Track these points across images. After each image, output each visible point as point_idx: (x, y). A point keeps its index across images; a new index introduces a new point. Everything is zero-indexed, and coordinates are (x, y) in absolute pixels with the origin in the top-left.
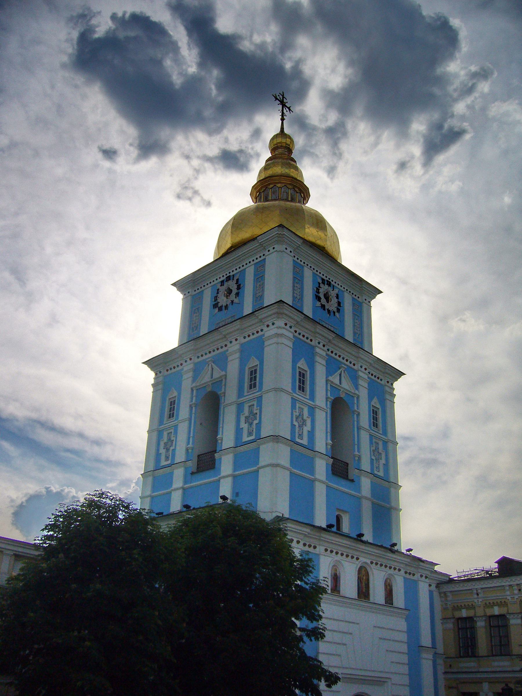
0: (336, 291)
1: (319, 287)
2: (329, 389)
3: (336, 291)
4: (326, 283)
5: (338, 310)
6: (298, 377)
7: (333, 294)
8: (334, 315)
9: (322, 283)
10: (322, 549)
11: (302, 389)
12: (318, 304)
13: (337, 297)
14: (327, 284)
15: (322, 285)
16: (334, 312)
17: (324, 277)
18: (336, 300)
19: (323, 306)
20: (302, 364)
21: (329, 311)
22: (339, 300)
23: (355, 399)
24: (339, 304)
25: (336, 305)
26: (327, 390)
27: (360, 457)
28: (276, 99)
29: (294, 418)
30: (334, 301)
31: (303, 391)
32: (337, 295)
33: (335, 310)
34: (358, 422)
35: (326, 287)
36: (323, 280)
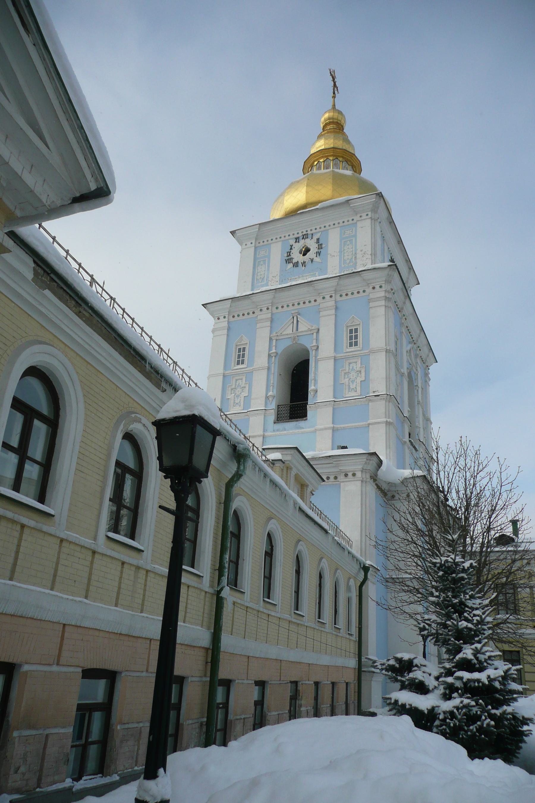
0: (315, 238)
2: (274, 344)
3: (315, 238)
7: (312, 244)
8: (312, 261)
9: (296, 242)
14: (303, 238)
16: (312, 260)
18: (317, 245)
19: (296, 265)
21: (304, 264)
22: (320, 243)
24: (320, 247)
32: (318, 240)
35: (302, 242)
36: (296, 239)
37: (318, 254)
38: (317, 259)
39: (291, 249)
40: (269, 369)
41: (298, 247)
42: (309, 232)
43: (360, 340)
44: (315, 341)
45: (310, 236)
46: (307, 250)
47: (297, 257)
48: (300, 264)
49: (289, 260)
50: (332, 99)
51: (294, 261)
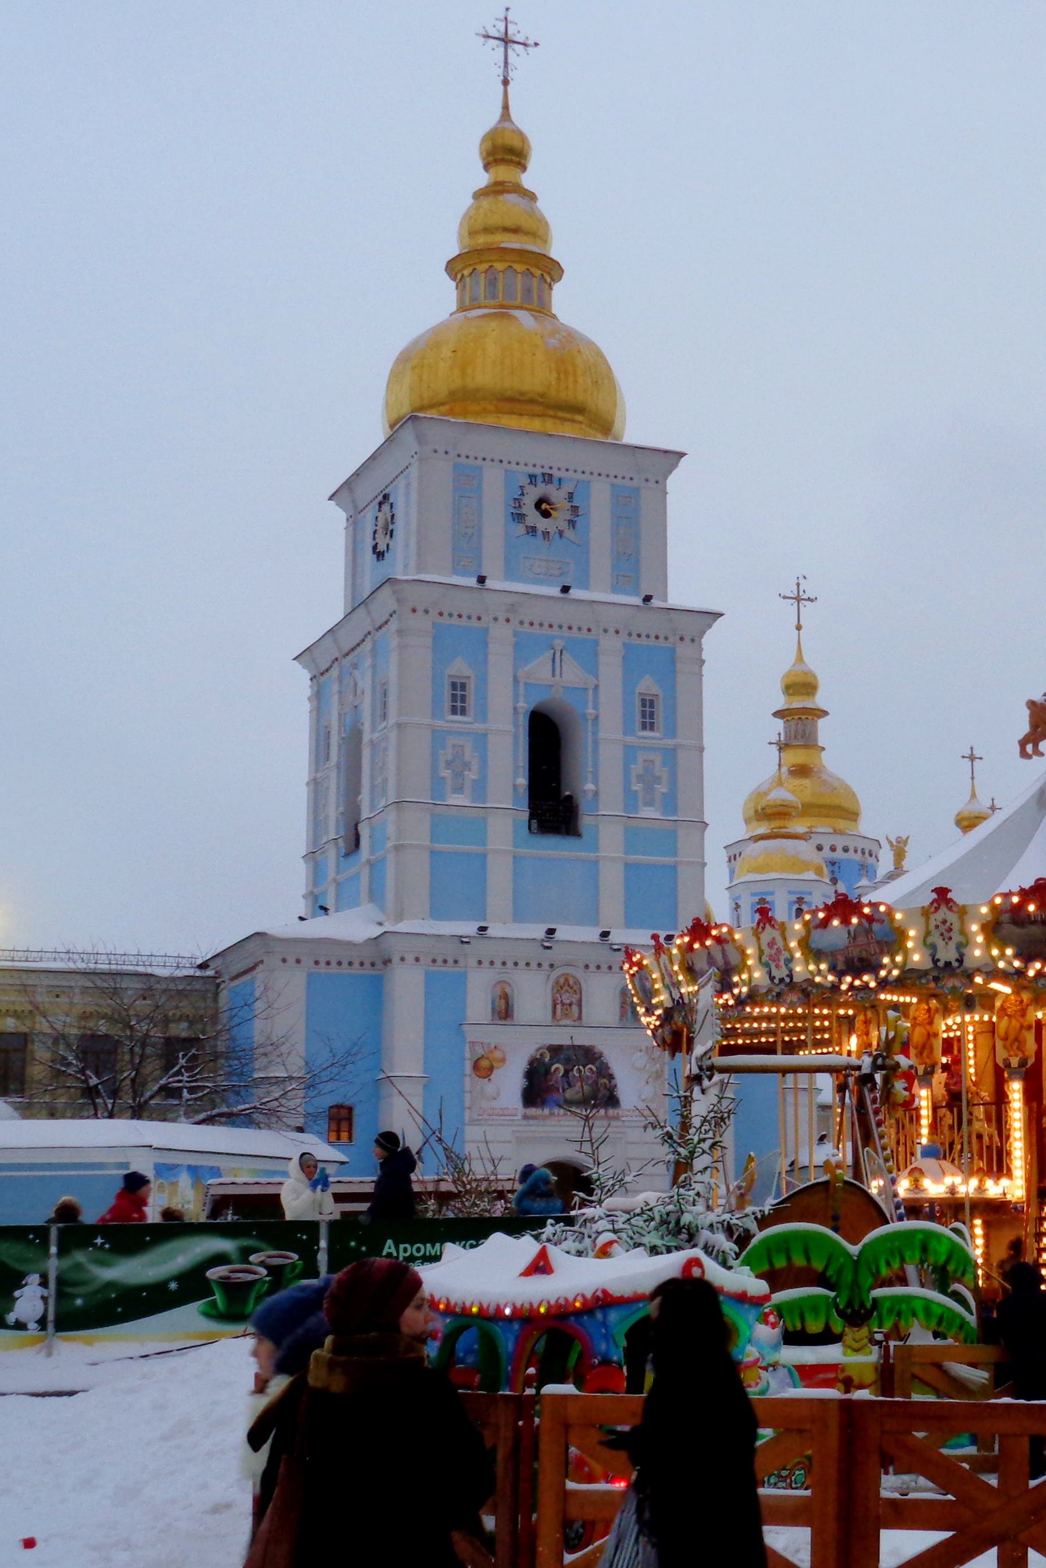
0: (568, 487)
1: (522, 494)
4: (540, 479)
5: (572, 523)
6: (447, 692)
7: (558, 496)
10: (472, 962)
11: (459, 707)
12: (521, 529)
13: (571, 496)
16: (561, 533)
17: (538, 471)
18: (568, 505)
19: (532, 530)
20: (459, 668)
21: (546, 534)
23: (591, 692)
24: (575, 509)
25: (568, 516)
26: (516, 697)
28: (487, 37)
29: (442, 764)
33: (563, 525)
34: (595, 733)
36: (532, 478)
37: (572, 523)
38: (569, 533)
39: (522, 494)
40: (516, 737)
43: (660, 719)
44: (590, 704)
45: (555, 481)
47: (534, 518)
48: (539, 533)
49: (519, 517)
50: (502, 87)
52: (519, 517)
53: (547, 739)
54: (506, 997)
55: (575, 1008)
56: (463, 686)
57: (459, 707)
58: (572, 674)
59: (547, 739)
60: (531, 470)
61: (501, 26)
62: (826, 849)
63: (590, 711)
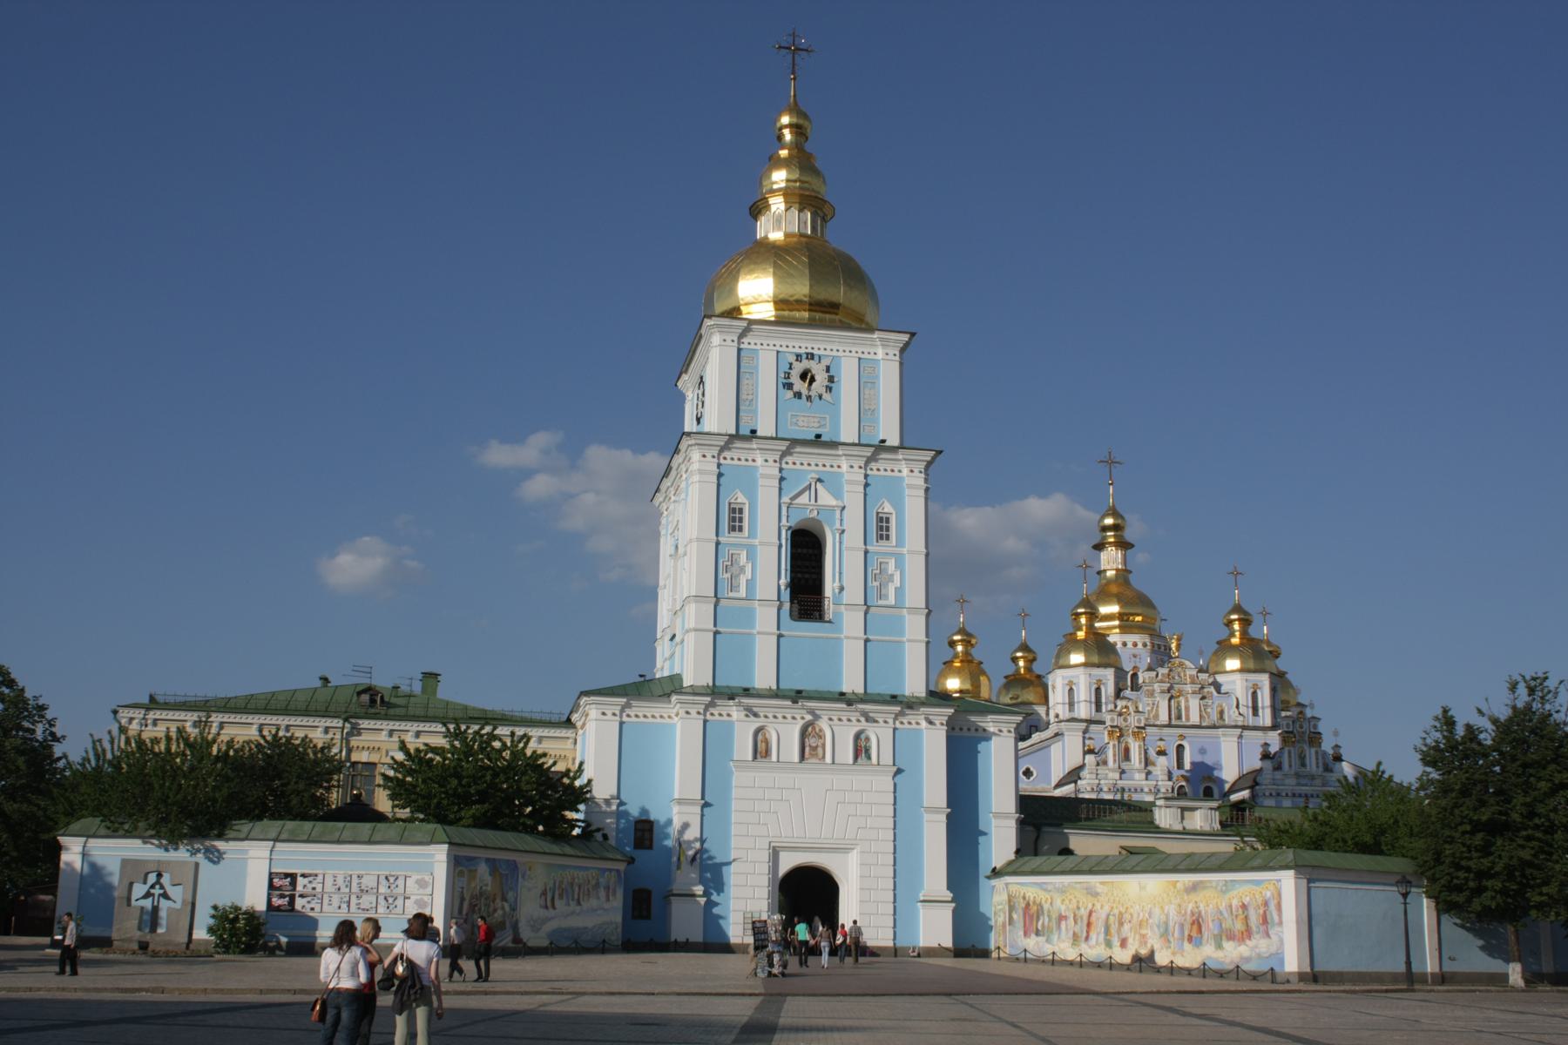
0: (825, 362)
5: (829, 389)
7: (818, 370)
12: (790, 394)
13: (828, 369)
15: (796, 365)
16: (820, 397)
17: (803, 351)
19: (798, 395)
21: (809, 398)
23: (838, 513)
24: (831, 379)
27: (842, 589)
30: (821, 378)
31: (741, 529)
35: (805, 364)
36: (799, 357)
38: (826, 396)
41: (799, 368)
42: (815, 352)
46: (813, 380)
47: (799, 385)
49: (789, 386)
51: (796, 388)
52: (789, 386)
53: (806, 550)
54: (767, 742)
55: (820, 750)
56: (741, 511)
57: (736, 523)
58: (826, 498)
59: (806, 550)
60: (797, 350)
61: (790, 39)
62: (1130, 645)
63: (838, 525)
